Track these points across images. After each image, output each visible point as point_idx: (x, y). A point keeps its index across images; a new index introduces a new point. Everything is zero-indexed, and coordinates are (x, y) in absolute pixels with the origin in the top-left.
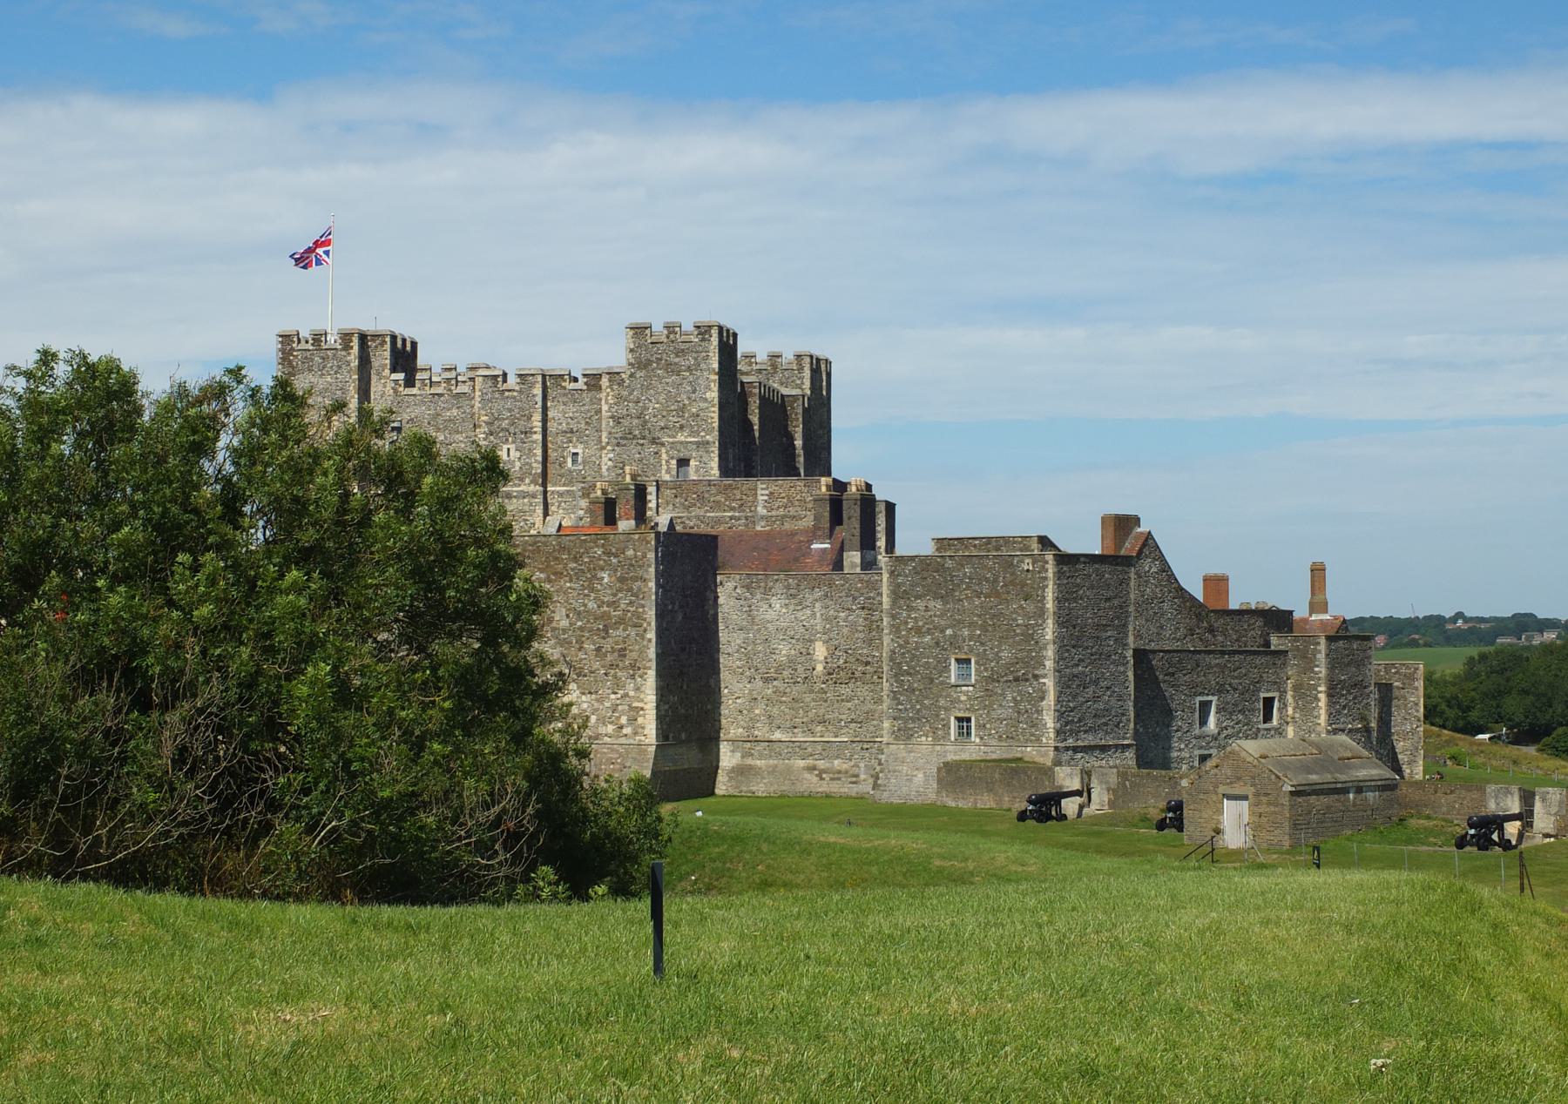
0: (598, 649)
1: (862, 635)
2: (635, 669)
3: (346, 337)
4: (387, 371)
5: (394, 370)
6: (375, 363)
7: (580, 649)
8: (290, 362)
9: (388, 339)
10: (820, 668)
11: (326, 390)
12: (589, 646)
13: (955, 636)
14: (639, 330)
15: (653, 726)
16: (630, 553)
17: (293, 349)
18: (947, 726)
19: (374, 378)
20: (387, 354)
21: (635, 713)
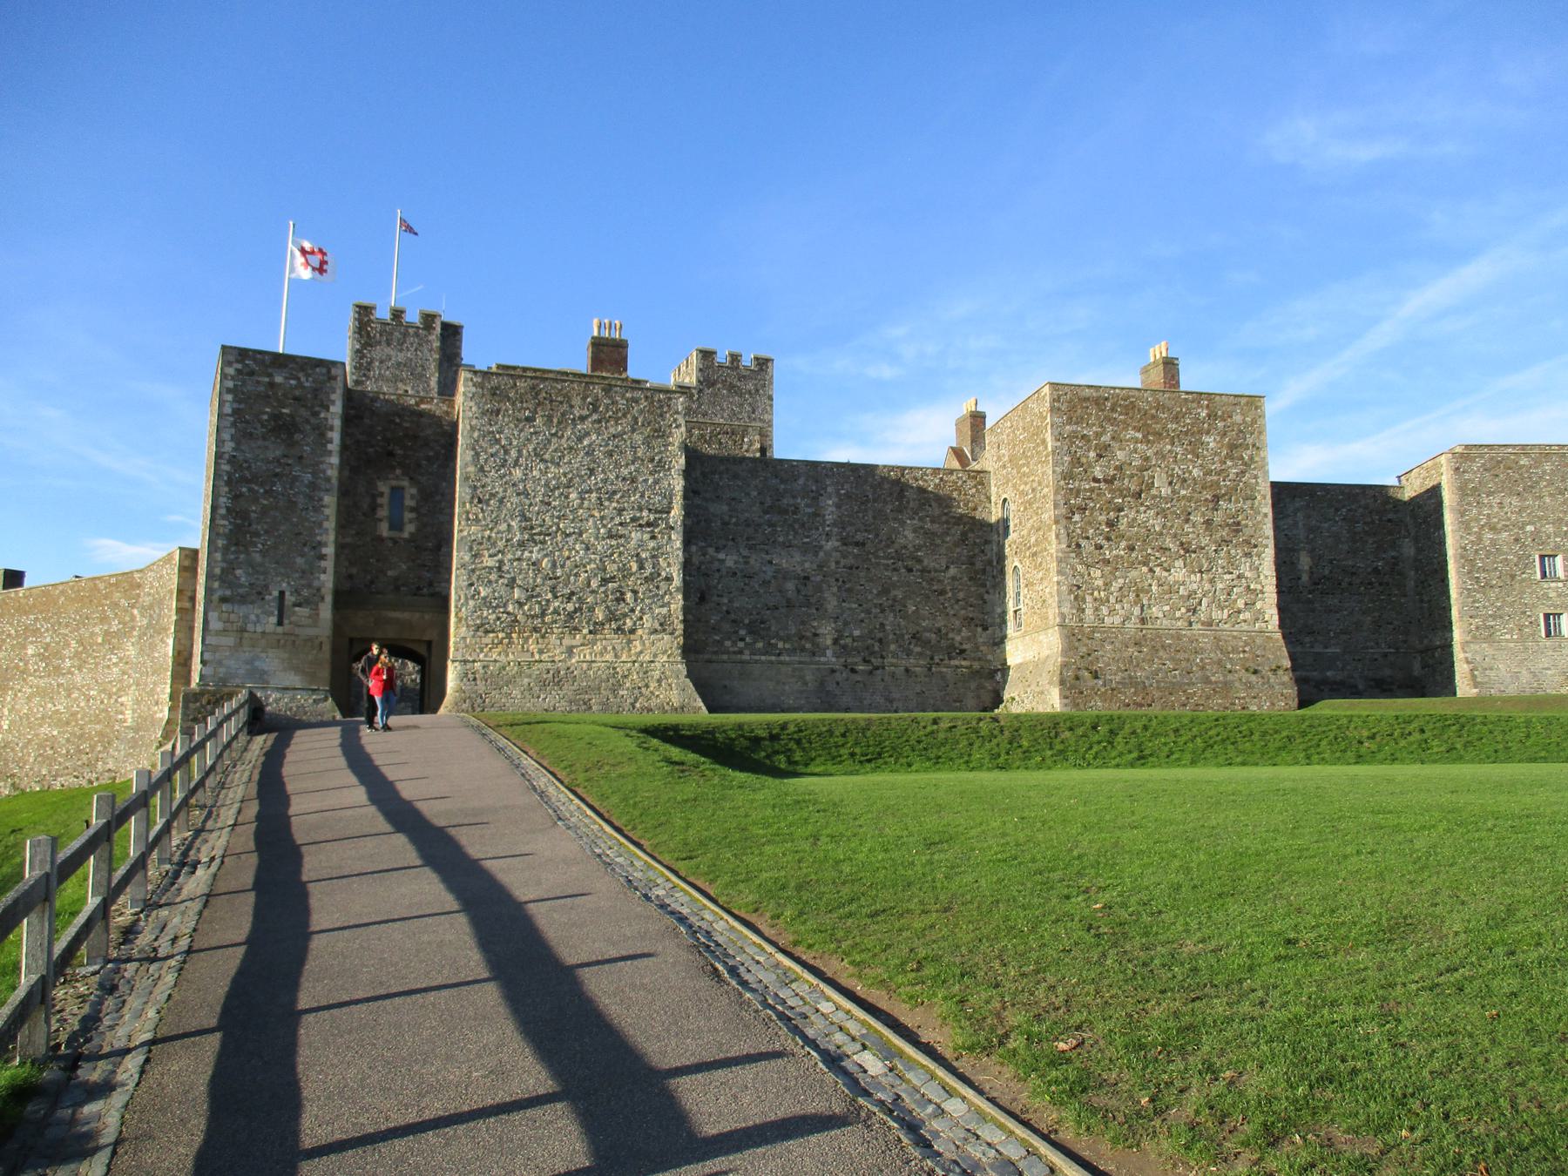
0: (1208, 523)
1: (1345, 547)
2: (1250, 547)
7: (1187, 521)
8: (368, 333)
10: (1305, 578)
12: (1197, 518)
13: (1537, 532)
14: (707, 355)
15: (1275, 611)
16: (1238, 418)
17: (370, 321)
18: (1535, 624)
21: (1253, 594)
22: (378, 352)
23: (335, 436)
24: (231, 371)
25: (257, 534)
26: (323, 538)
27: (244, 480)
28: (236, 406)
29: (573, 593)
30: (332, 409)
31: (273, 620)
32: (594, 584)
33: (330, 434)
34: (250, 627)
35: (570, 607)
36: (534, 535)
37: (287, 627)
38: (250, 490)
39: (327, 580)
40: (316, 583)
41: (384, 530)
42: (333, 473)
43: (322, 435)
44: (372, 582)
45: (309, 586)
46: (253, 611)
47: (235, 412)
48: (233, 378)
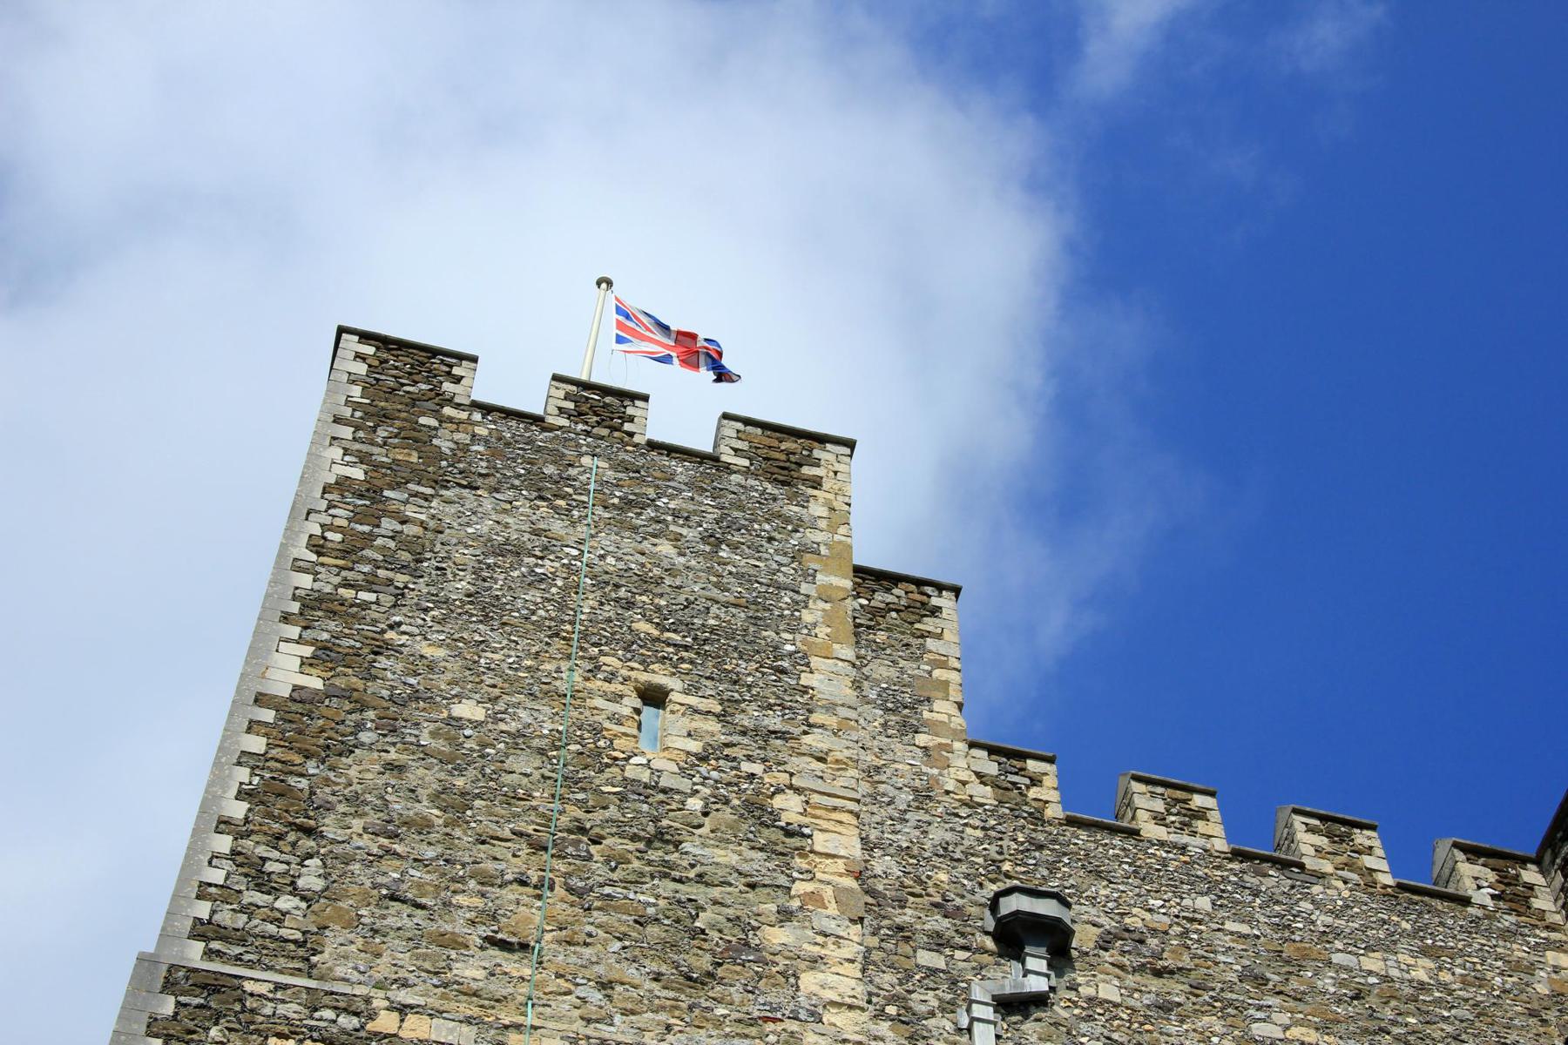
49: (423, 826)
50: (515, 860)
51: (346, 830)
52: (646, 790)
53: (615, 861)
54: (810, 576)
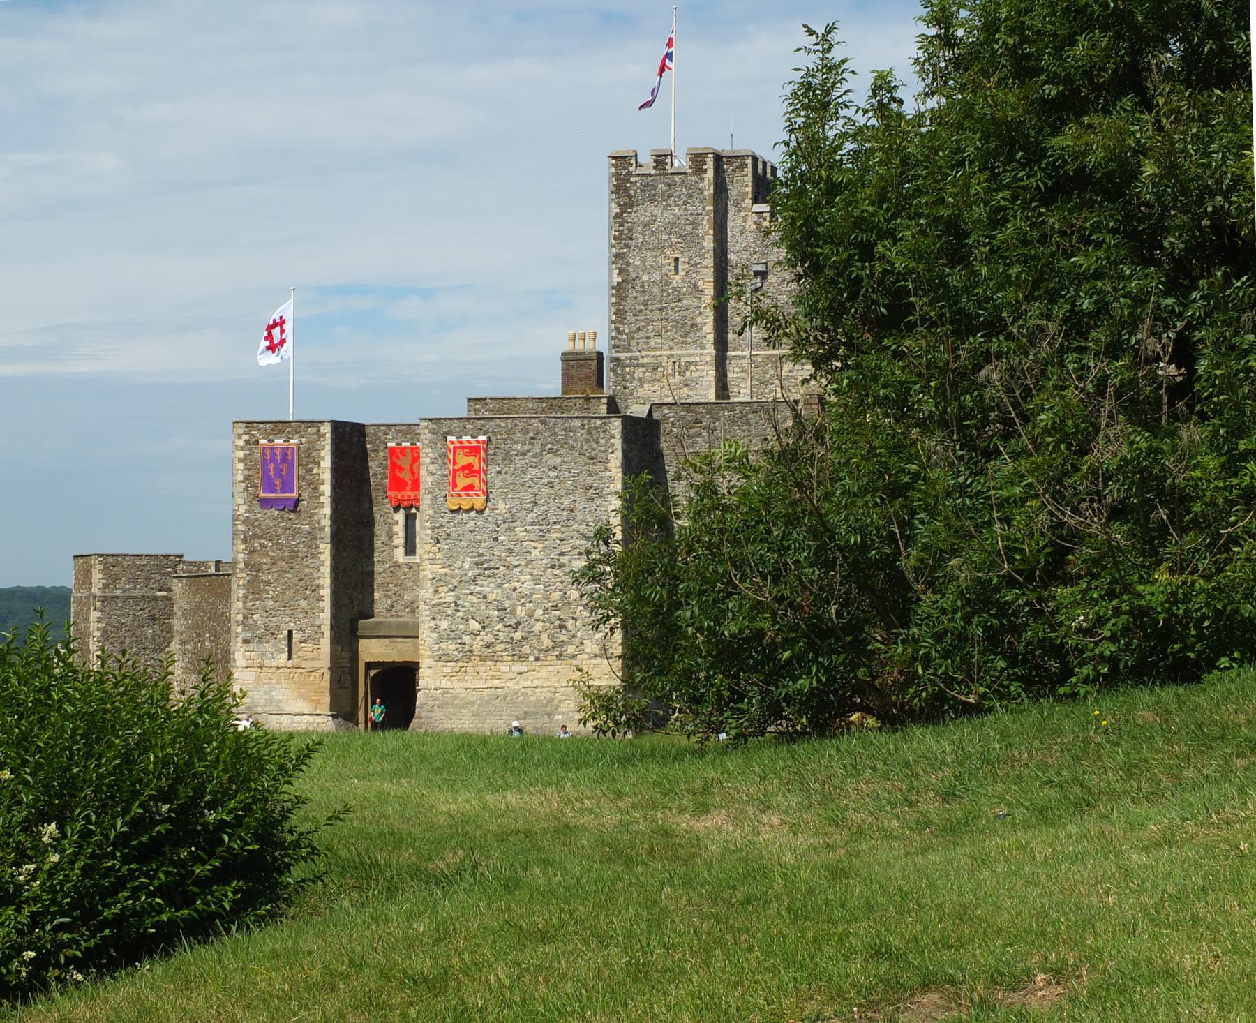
3: (698, 159)
4: (748, 202)
5: (756, 200)
6: (733, 191)
9: (749, 161)
11: (673, 225)
17: (629, 174)
19: (731, 211)
20: (748, 180)
22: (640, 214)
23: (326, 489)
24: (241, 443)
25: (268, 583)
26: (321, 582)
27: (255, 536)
28: (246, 472)
29: (519, 624)
30: (323, 464)
31: (286, 655)
32: (540, 612)
33: (322, 488)
34: (267, 663)
35: (518, 636)
36: (485, 568)
37: (294, 661)
38: (261, 545)
39: (325, 618)
40: (318, 623)
41: (399, 555)
42: (326, 522)
43: (316, 489)
44: (392, 606)
45: (312, 625)
46: (269, 648)
47: (246, 478)
48: (242, 449)
49: (641, 311)
50: (657, 315)
51: (630, 317)
52: (675, 289)
53: (673, 309)
54: (704, 208)
